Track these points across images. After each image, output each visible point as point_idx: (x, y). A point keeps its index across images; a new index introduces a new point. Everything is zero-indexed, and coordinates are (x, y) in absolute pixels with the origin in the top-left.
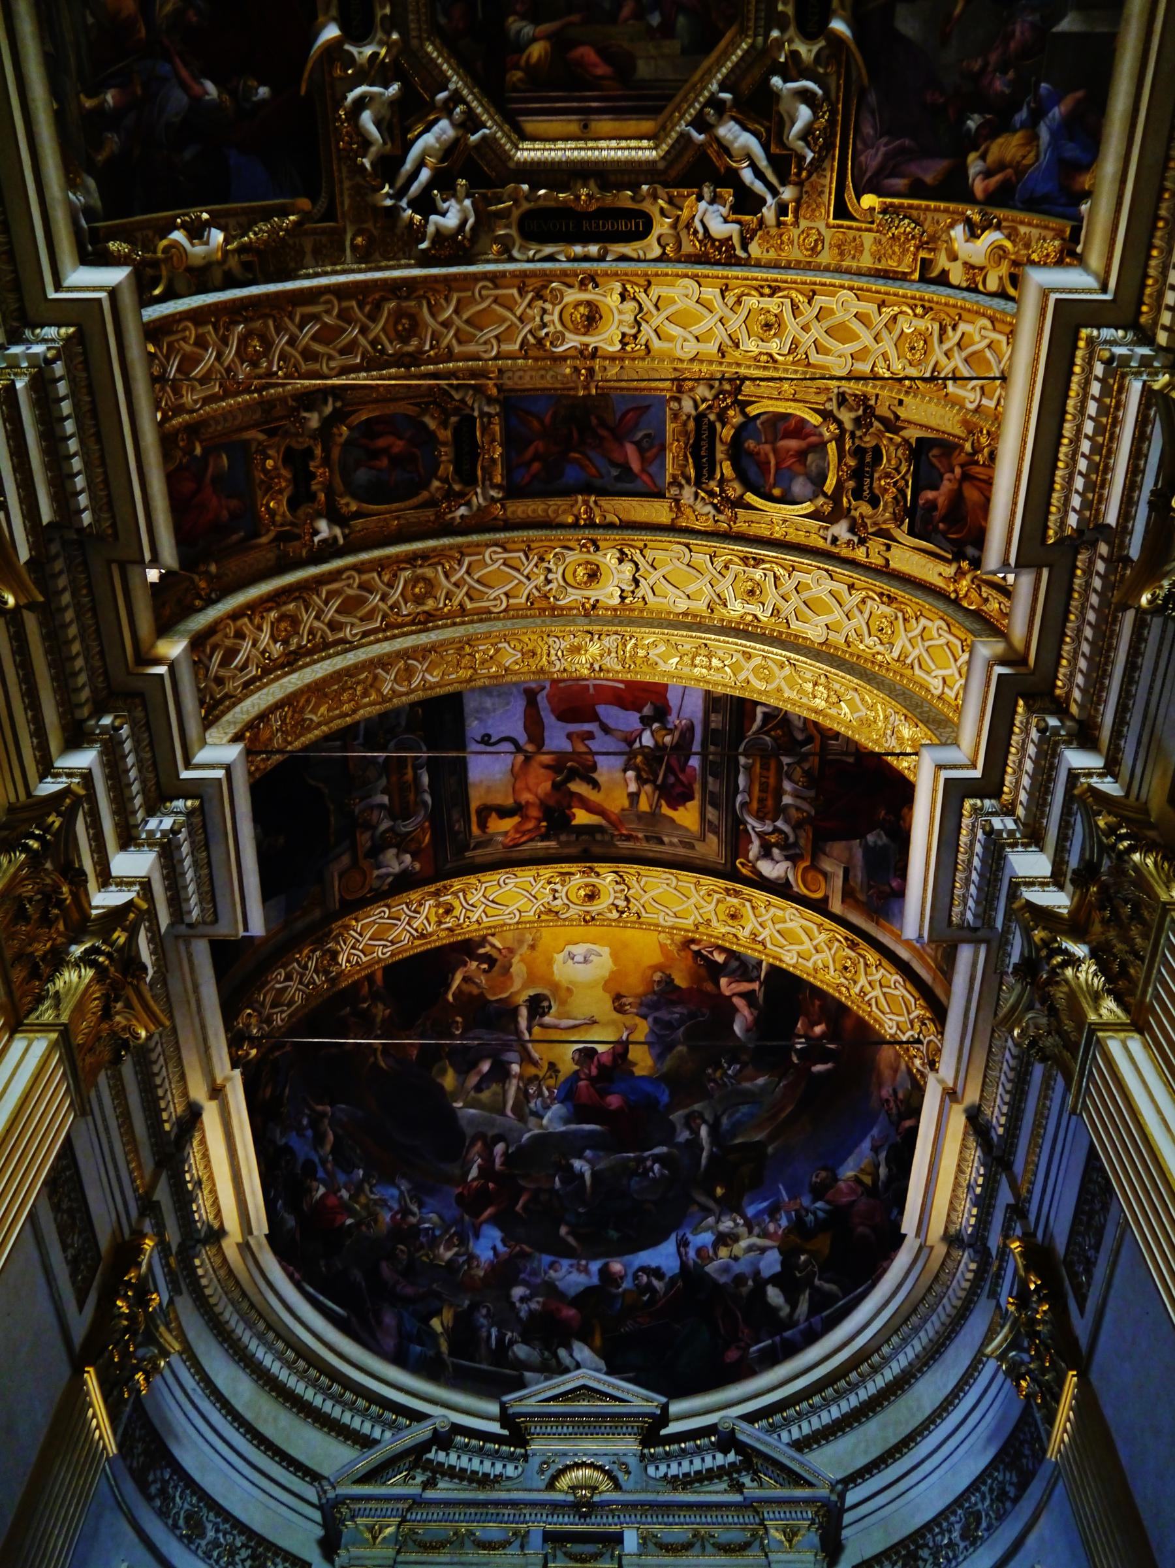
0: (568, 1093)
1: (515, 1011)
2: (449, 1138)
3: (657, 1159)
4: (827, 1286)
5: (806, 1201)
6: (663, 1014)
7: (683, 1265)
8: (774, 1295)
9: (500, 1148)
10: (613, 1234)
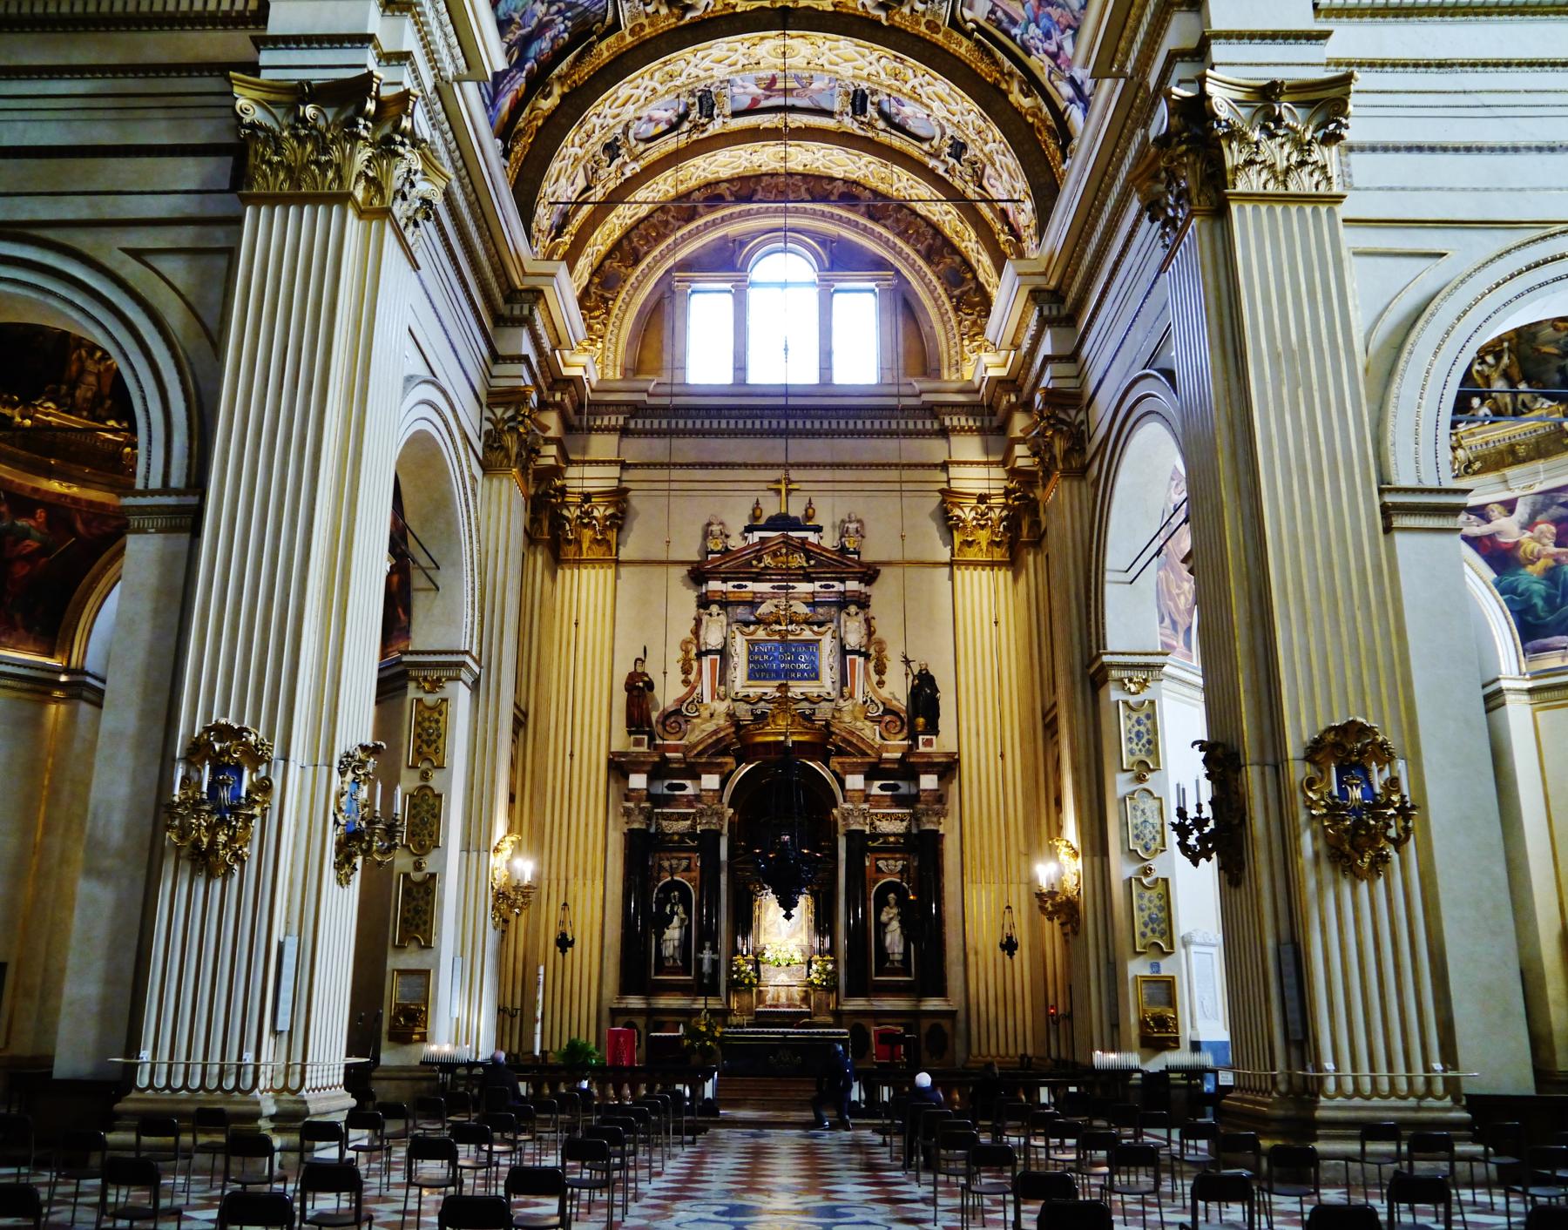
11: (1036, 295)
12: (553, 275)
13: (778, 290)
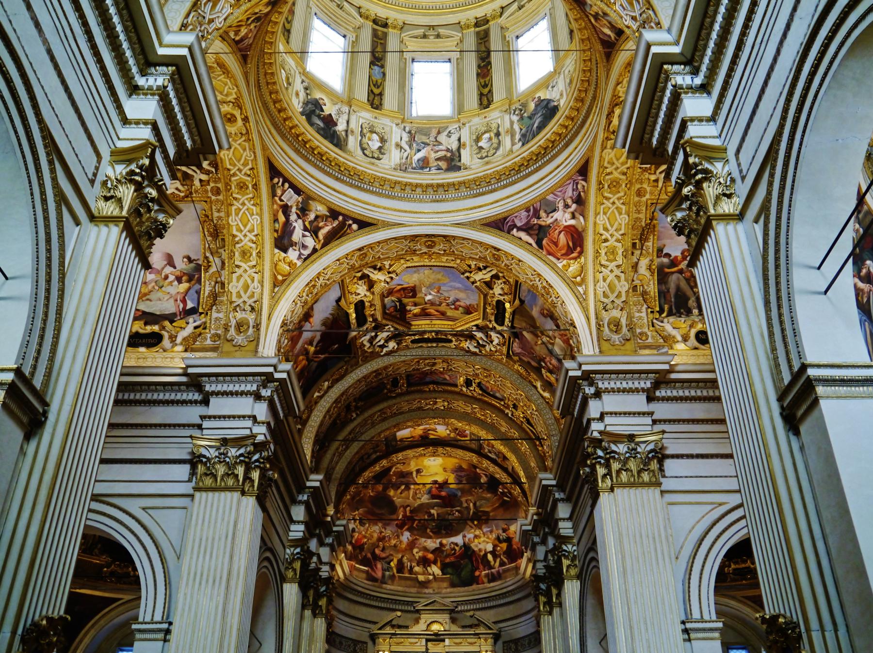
0: (429, 492)
1: (412, 473)
2: (392, 507)
3: (457, 511)
4: (505, 560)
5: (501, 531)
6: (459, 474)
7: (464, 543)
8: (490, 557)
9: (408, 509)
10: (444, 532)
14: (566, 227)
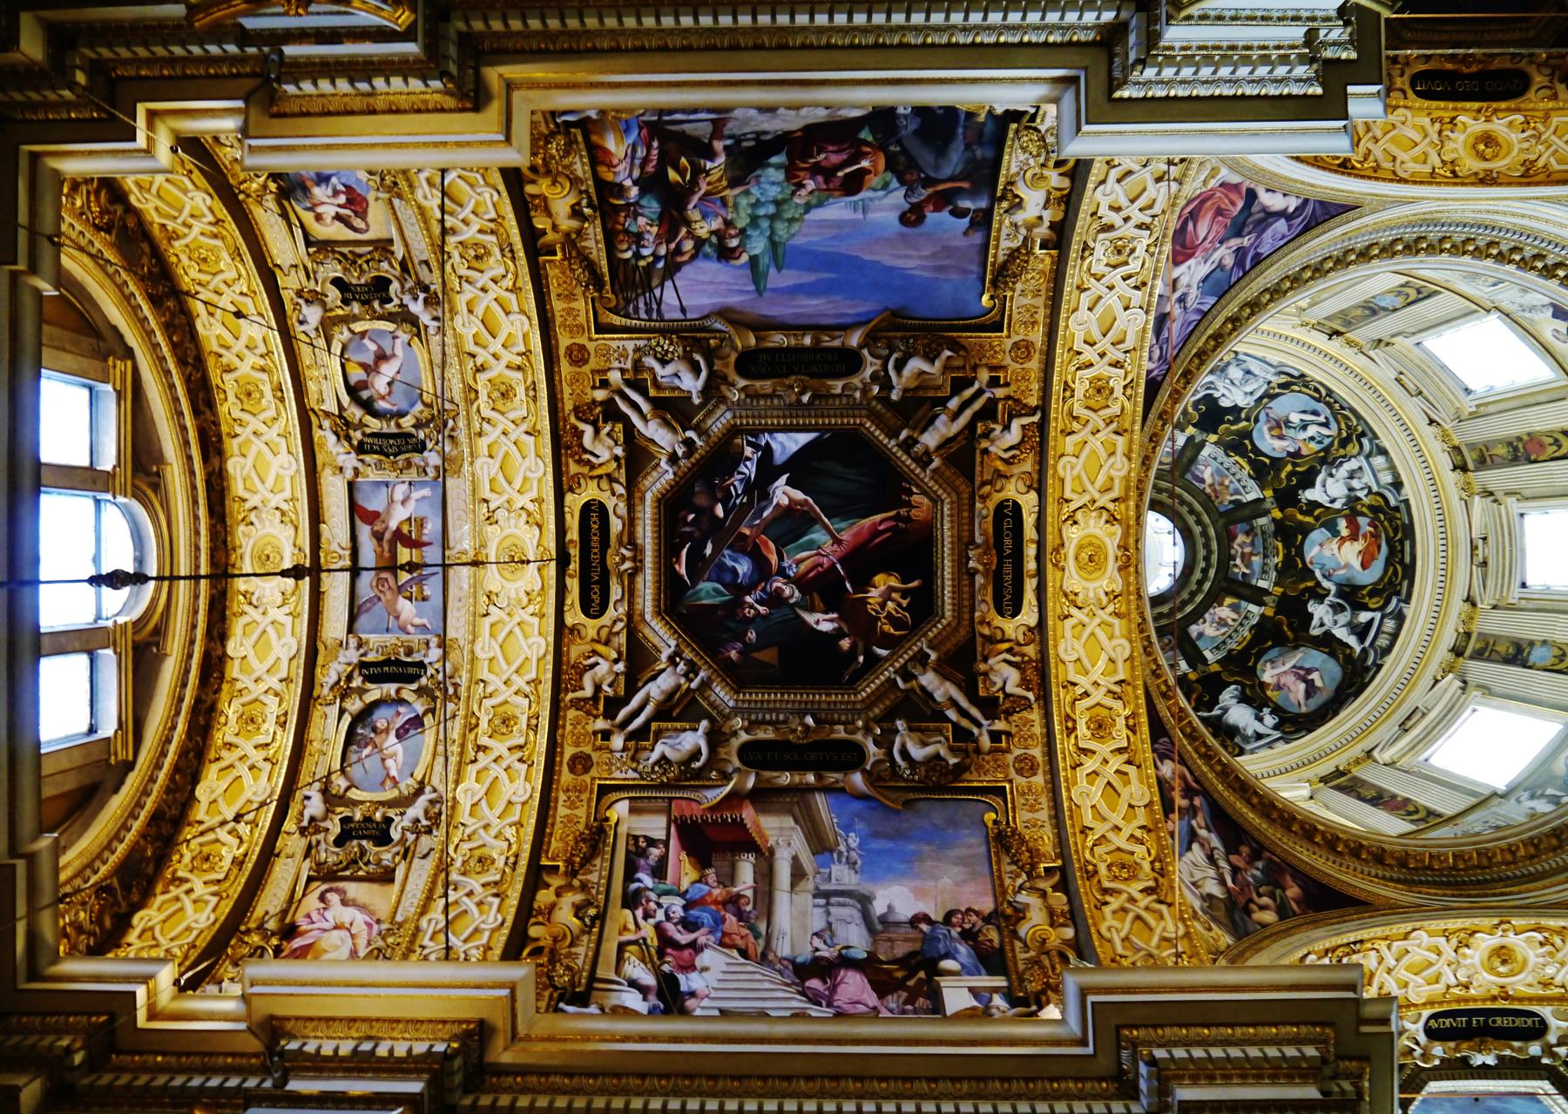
11: (477, 1034)
12: (508, 139)
13: (93, 550)
14: (1191, 256)
